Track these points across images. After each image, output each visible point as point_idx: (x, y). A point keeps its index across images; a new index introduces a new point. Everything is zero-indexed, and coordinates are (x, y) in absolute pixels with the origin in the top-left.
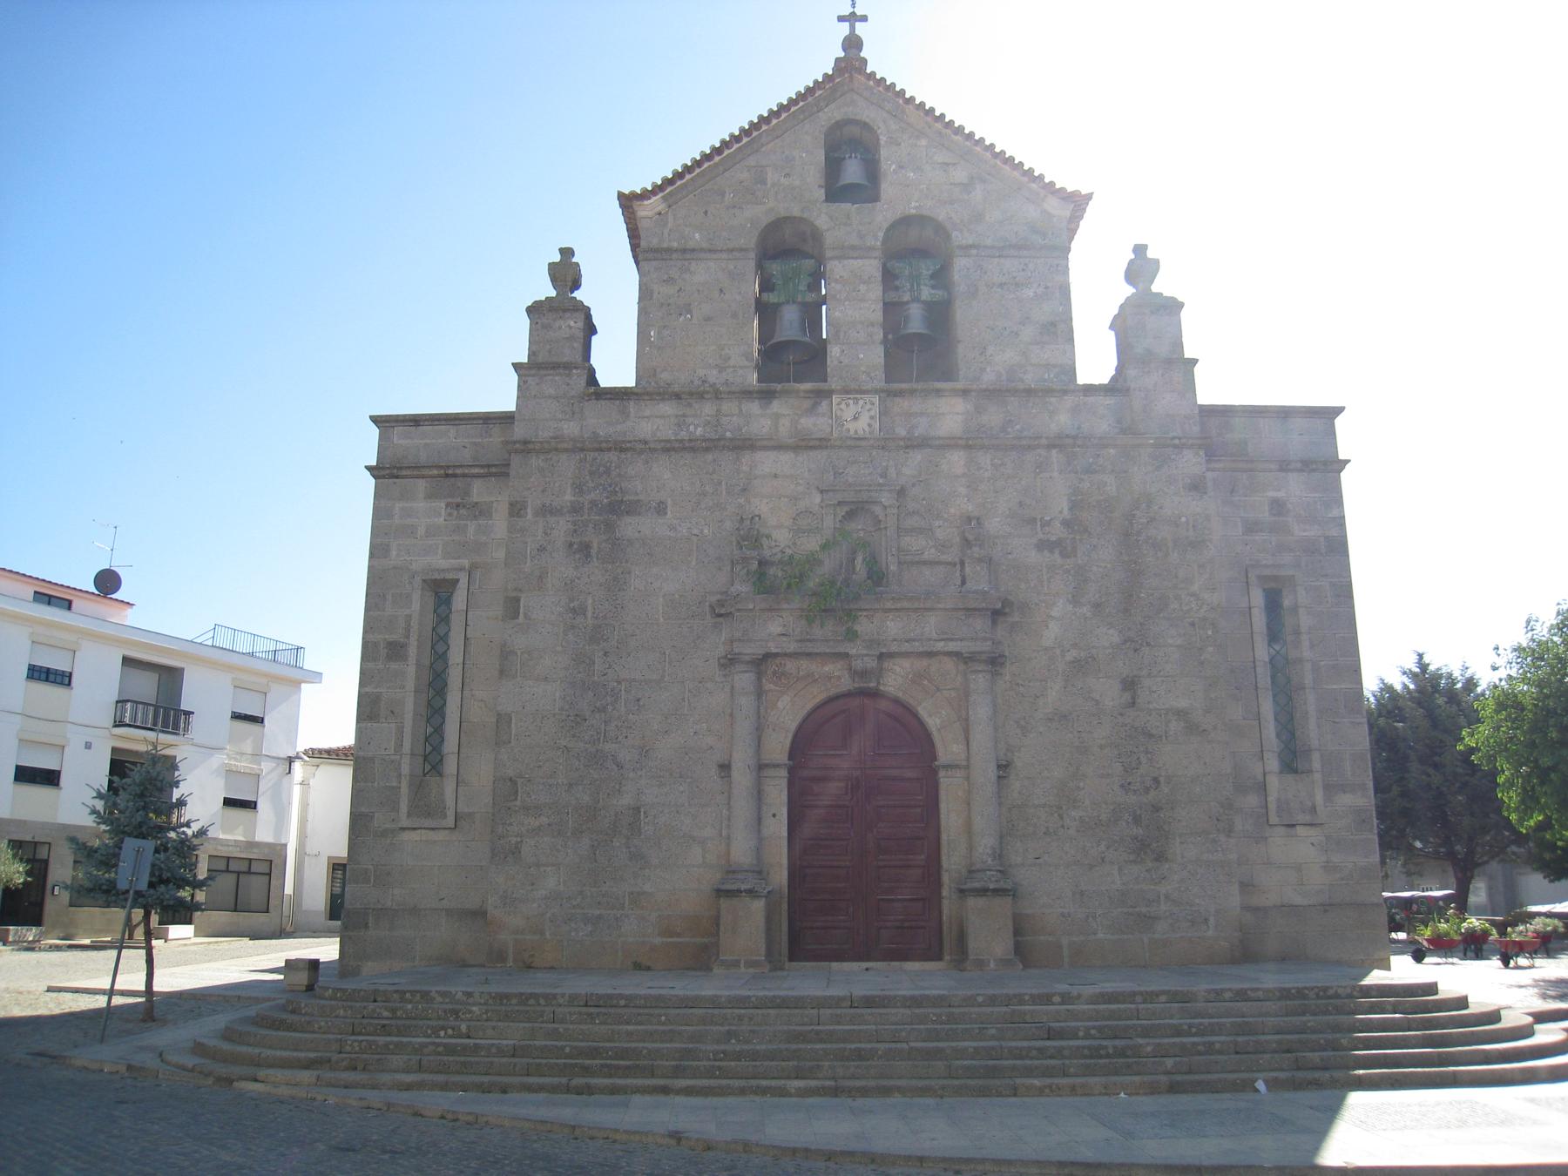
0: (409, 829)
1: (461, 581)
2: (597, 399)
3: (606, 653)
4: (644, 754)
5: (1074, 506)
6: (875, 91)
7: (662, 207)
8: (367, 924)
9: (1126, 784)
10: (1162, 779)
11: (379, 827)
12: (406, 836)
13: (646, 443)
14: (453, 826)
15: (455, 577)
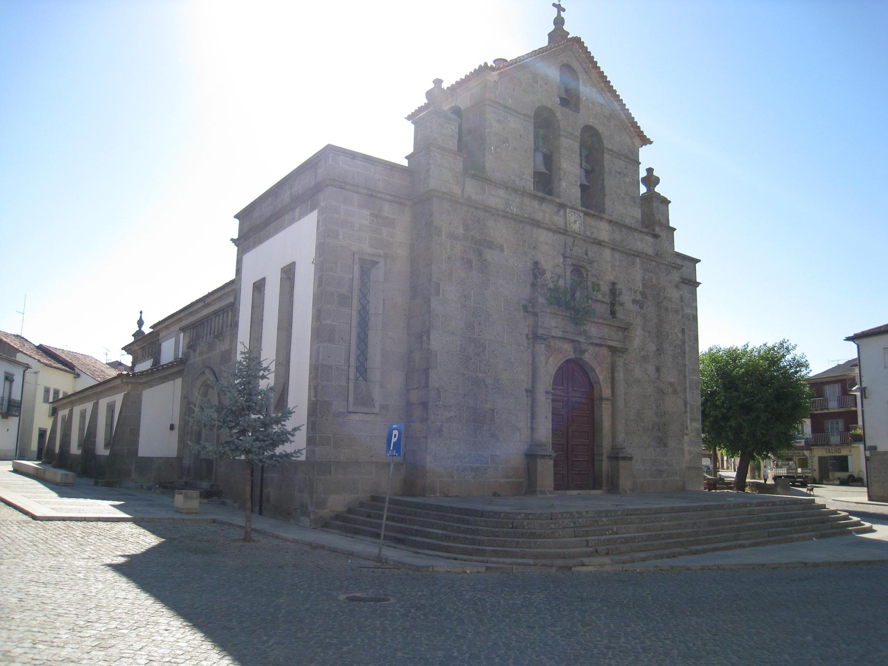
0: (353, 412)
1: (380, 263)
2: (472, 178)
3: (480, 323)
4: (496, 381)
5: (644, 285)
6: (581, 55)
7: (496, 78)
8: (330, 471)
10: (666, 412)
11: (336, 410)
12: (353, 417)
13: (498, 210)
14: (349, 411)
15: (378, 260)
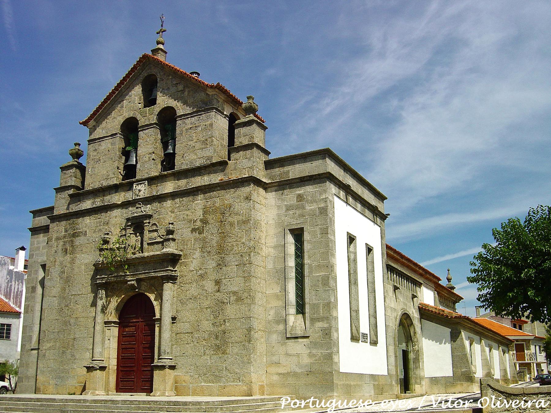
5: (205, 213)
9: (214, 323)
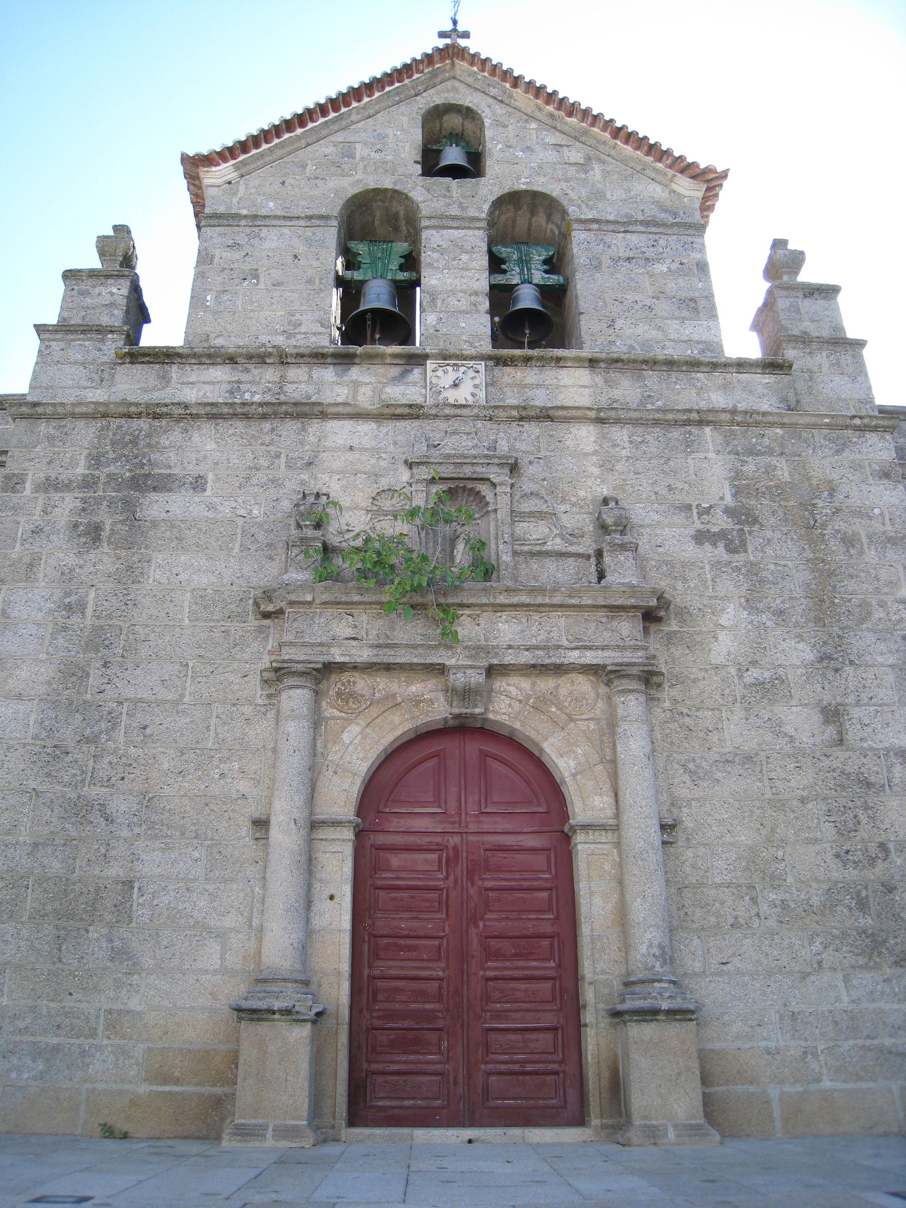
2: (132, 363)
3: (106, 663)
5: (737, 492)
7: (233, 176)
9: (843, 854)
10: (891, 846)
13: (186, 407)
